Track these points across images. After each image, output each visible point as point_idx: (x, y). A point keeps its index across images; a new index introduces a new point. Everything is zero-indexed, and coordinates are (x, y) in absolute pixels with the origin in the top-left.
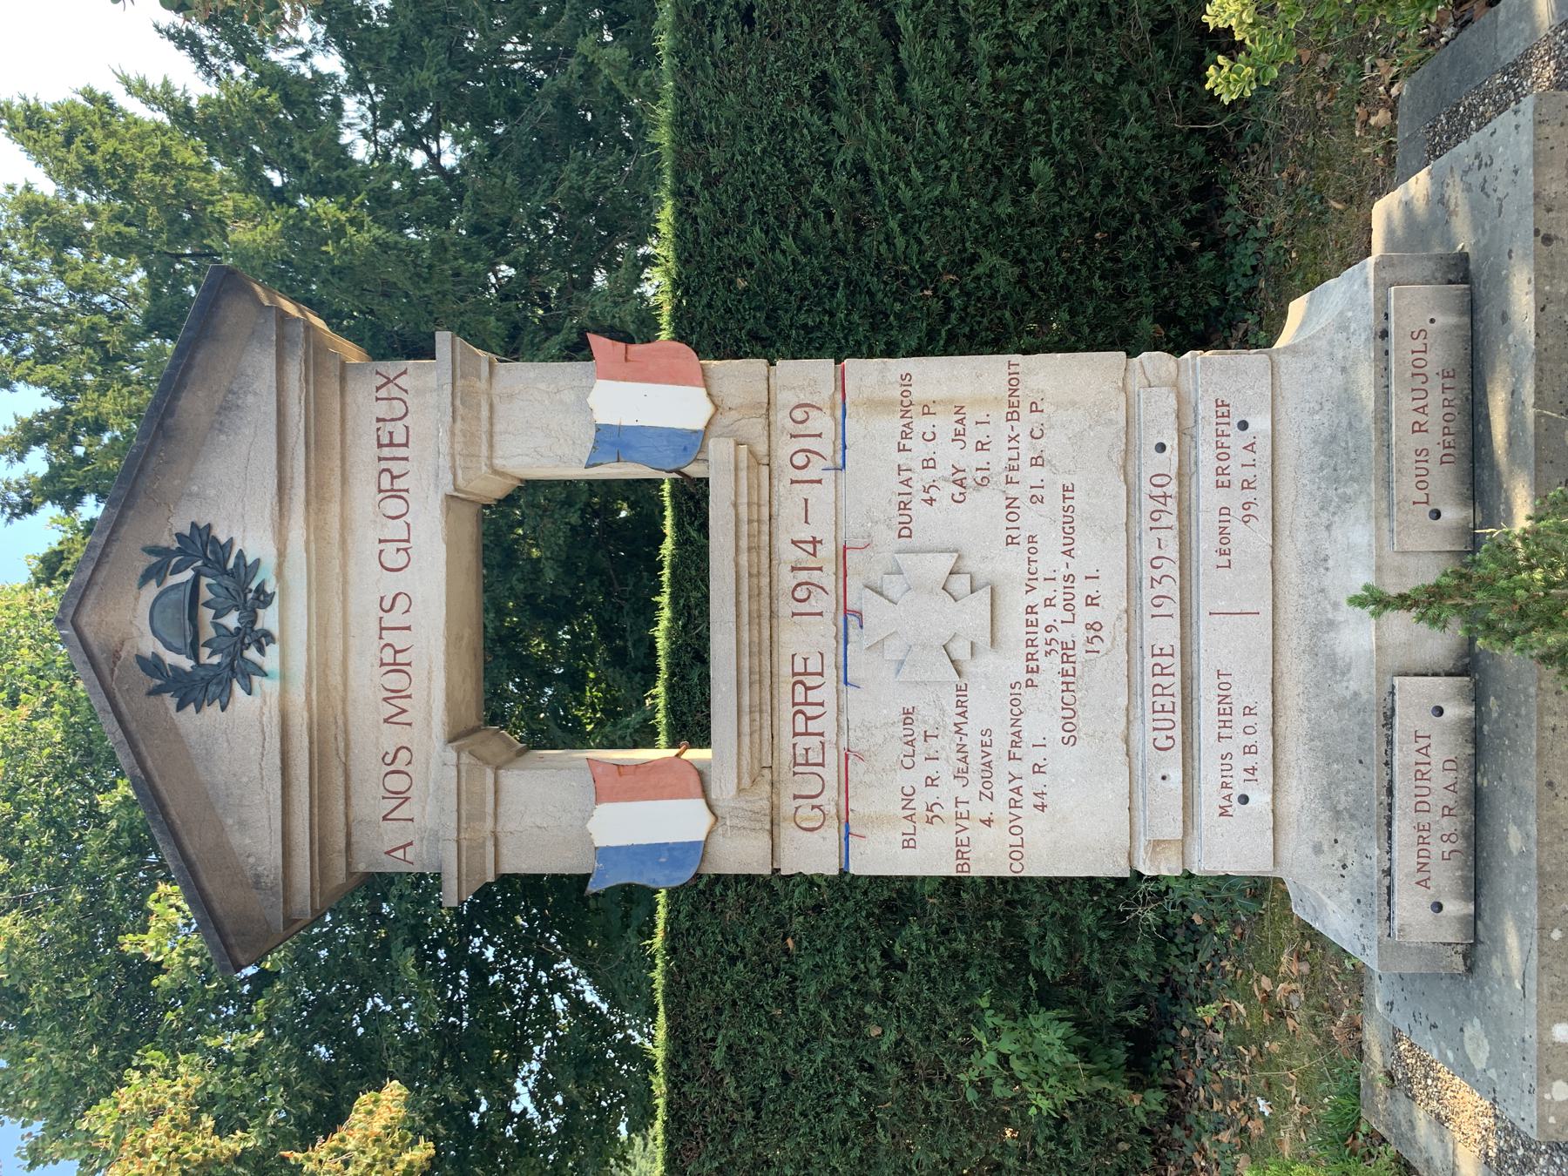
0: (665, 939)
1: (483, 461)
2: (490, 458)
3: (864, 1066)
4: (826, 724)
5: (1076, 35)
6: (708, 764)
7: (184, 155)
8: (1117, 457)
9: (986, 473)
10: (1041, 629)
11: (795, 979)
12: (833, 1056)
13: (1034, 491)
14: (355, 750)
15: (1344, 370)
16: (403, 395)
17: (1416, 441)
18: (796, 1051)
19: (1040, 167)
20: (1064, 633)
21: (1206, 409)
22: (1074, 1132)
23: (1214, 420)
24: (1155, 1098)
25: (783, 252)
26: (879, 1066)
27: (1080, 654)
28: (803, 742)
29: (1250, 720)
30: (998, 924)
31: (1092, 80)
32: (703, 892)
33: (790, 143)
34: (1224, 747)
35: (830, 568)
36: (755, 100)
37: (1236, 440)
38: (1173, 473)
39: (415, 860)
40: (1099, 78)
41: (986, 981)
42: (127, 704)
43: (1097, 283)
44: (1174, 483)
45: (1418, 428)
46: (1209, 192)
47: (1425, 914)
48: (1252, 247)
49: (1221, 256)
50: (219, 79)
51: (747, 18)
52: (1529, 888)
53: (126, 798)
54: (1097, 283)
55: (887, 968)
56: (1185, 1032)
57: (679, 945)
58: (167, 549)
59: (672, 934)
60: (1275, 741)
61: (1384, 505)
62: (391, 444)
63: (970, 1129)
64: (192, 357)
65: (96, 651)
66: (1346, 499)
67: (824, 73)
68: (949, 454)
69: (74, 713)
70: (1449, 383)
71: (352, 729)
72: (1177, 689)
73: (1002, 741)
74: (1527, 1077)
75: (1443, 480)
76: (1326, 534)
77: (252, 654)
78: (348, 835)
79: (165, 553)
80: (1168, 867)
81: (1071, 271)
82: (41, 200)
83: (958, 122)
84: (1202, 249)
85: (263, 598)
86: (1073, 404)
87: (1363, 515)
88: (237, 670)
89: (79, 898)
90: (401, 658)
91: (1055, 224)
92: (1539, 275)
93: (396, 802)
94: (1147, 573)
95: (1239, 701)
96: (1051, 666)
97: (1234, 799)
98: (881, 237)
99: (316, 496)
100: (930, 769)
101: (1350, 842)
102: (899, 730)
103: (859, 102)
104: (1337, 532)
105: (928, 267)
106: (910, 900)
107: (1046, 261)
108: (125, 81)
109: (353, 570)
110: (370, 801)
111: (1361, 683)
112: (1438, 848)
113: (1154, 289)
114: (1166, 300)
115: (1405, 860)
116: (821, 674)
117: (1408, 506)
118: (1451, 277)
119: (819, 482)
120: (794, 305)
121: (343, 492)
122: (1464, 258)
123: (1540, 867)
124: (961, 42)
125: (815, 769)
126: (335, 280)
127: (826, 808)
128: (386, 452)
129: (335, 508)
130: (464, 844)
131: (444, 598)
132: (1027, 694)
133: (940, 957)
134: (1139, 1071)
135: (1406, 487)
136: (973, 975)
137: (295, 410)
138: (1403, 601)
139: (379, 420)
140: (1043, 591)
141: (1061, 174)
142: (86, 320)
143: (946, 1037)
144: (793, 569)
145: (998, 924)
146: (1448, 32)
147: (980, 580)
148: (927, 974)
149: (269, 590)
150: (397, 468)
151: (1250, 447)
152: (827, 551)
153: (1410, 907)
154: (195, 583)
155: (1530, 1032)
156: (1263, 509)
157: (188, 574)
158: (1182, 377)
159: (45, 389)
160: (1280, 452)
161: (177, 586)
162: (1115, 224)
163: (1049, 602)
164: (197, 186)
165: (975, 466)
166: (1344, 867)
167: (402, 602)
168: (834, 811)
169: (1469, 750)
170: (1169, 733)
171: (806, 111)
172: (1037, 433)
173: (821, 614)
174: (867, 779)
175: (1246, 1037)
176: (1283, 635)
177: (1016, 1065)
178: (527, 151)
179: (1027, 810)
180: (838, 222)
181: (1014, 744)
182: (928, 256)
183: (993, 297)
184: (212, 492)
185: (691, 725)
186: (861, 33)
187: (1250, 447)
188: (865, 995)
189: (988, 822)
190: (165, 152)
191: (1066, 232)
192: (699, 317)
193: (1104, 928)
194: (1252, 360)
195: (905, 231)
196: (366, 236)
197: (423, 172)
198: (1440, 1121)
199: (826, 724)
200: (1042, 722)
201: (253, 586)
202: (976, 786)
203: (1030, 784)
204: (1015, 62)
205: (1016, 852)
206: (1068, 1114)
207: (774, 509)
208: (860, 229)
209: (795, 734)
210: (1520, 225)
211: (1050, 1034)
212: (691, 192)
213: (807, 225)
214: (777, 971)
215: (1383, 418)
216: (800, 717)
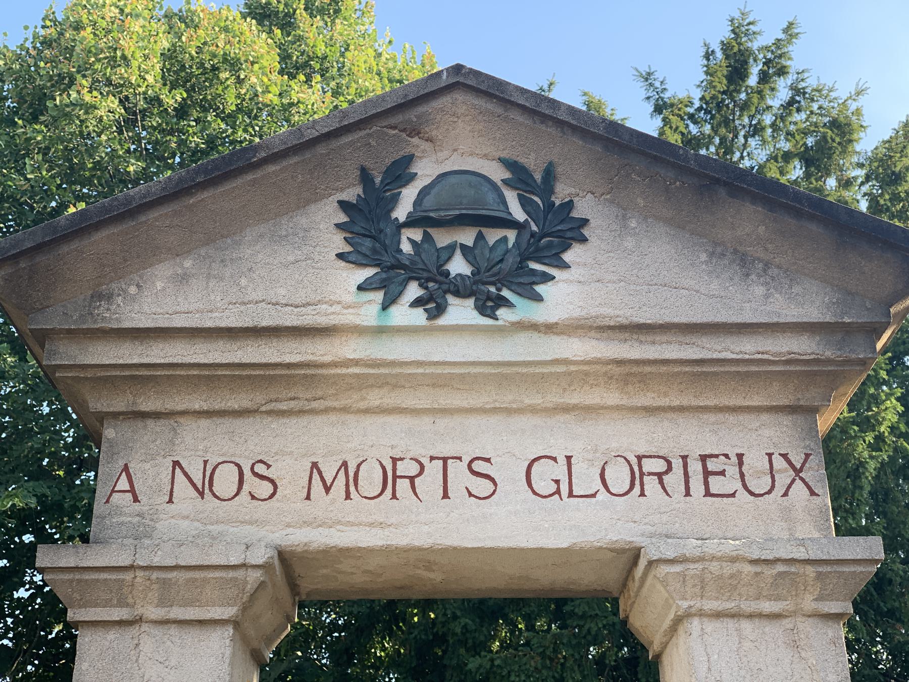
1: (697, 604)
2: (701, 614)
14: (275, 424)
16: (779, 490)
39: (113, 506)
42: (352, 143)
58: (552, 192)
62: (707, 474)
64: (812, 218)
65: (421, 109)
71: (304, 420)
77: (413, 291)
78: (156, 415)
85: (489, 305)
89: (131, 169)
90: (403, 485)
93: (198, 479)
99: (630, 373)
110: (199, 444)
121: (634, 410)
128: (695, 467)
129: (613, 398)
130: (128, 576)
131: (489, 544)
137: (747, 347)
139: (740, 456)
149: (501, 312)
150: (674, 480)
154: (509, 223)
157: (519, 214)
161: (504, 203)
167: (482, 487)
196: (866, 454)
201: (506, 293)
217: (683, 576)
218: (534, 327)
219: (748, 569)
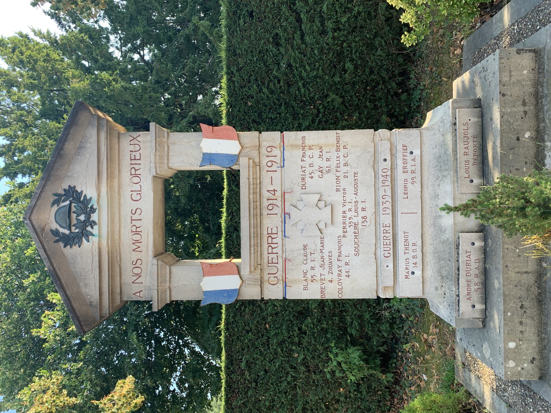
0: (225, 325)
1: (166, 164)
2: (168, 164)
3: (292, 367)
4: (279, 250)
5: (360, 22)
6: (240, 263)
7: (55, 56)
8: (371, 163)
9: (329, 168)
10: (347, 219)
11: (269, 338)
12: (282, 364)
13: (345, 174)
14: (123, 260)
15: (443, 135)
16: (139, 143)
17: (465, 158)
18: (269, 362)
19: (349, 65)
20: (355, 220)
21: (400, 147)
22: (363, 388)
23: (402, 151)
24: (390, 376)
25: (263, 93)
26: (298, 367)
27: (360, 226)
28: (271, 256)
29: (414, 247)
30: (337, 318)
31: (366, 36)
32: (237, 309)
33: (265, 57)
34: (407, 256)
35: (279, 199)
36: (254, 42)
37: (409, 157)
38: (389, 168)
40: (368, 36)
41: (333, 337)
42: (47, 245)
43: (368, 104)
44: (390, 171)
45: (466, 154)
46: (404, 74)
47: (470, 309)
48: (419, 92)
49: (409, 95)
50: (66, 29)
51: (251, 15)
52: (501, 299)
53: (33, 281)
54: (368, 104)
55: (300, 334)
56: (400, 354)
57: (230, 327)
58: (61, 194)
59: (227, 324)
60: (423, 254)
61: (456, 178)
62: (135, 159)
63: (328, 388)
64: (69, 131)
65: (37, 227)
66: (444, 176)
67: (277, 34)
68: (317, 162)
69: (14, 251)
70: (475, 139)
71: (122, 253)
72: (391, 237)
73: (335, 254)
74: (501, 360)
75: (474, 170)
76: (438, 188)
77: (89, 228)
78: (121, 288)
79: (59, 195)
80: (389, 295)
81: (359, 100)
82: (3, 71)
83: (321, 50)
84: (403, 92)
85: (93, 210)
86: (357, 146)
87: (449, 182)
88: (84, 234)
90: (138, 230)
91: (354, 84)
92: (501, 107)
93: (136, 277)
94: (381, 200)
95: (411, 241)
96: (351, 230)
97: (410, 273)
98: (296, 88)
99: (110, 177)
100: (312, 264)
101: (447, 286)
102: (302, 252)
103: (289, 43)
104: (441, 187)
105: (312, 98)
106: (308, 310)
107: (351, 96)
108: (34, 31)
109: (122, 202)
110: (128, 277)
111: (449, 235)
112: (473, 288)
113: (387, 106)
114: (391, 109)
115: (463, 291)
116: (277, 234)
117: (463, 178)
118: (476, 106)
119: (276, 171)
120: (267, 111)
121: (119, 175)
122: (479, 100)
123: (504, 292)
124: (322, 24)
125: (275, 265)
126: (108, 100)
127: (279, 277)
128: (133, 162)
130: (160, 290)
131: (152, 210)
132: (343, 240)
133: (318, 329)
134: (385, 367)
135: (462, 173)
136: (329, 335)
137: (103, 149)
138: (456, 209)
139: (131, 151)
140: (348, 206)
141: (356, 68)
142: (19, 113)
143: (320, 357)
144: (268, 199)
145: (337, 318)
146: (478, 25)
147: (328, 203)
148: (313, 335)
149: (95, 207)
150: (137, 167)
151: (414, 160)
152: (279, 194)
153: (465, 306)
154: (70, 205)
155: (502, 345)
156: (418, 180)
157: (68, 202)
158: (392, 138)
159: (4, 137)
160: (423, 161)
161: (64, 206)
162: (374, 84)
163: (350, 210)
164: (59, 67)
165: (326, 166)
166: (445, 294)
167: (139, 211)
168: (281, 278)
169: (483, 256)
170: (389, 252)
171: (271, 46)
172: (346, 156)
173: (276, 214)
174: (292, 268)
175: (419, 355)
176: (425, 220)
177: (343, 365)
178: (175, 55)
179: (343, 277)
180: (282, 83)
181: (339, 256)
182: (312, 95)
183: (334, 108)
184: (76, 175)
185: (234, 251)
186: (289, 21)
187: (414, 160)
188: (293, 343)
189: (331, 281)
190: (48, 55)
191: (357, 87)
192: (235, 115)
193: (372, 319)
194: (413, 132)
195: (304, 87)
197: (138, 61)
198: (479, 378)
199: (279, 250)
200: (348, 248)
201: (89, 206)
202: (327, 270)
203: (344, 269)
204: (340, 30)
205: (340, 291)
206: (361, 382)
207: (261, 180)
208: (289, 86)
209: (268, 254)
210: (495, 90)
211: (355, 354)
212: (233, 73)
213: (271, 84)
214: (263, 335)
215: (455, 151)
216: (270, 248)
217: (160, 167)
218: (98, 199)
219: (157, 153)
